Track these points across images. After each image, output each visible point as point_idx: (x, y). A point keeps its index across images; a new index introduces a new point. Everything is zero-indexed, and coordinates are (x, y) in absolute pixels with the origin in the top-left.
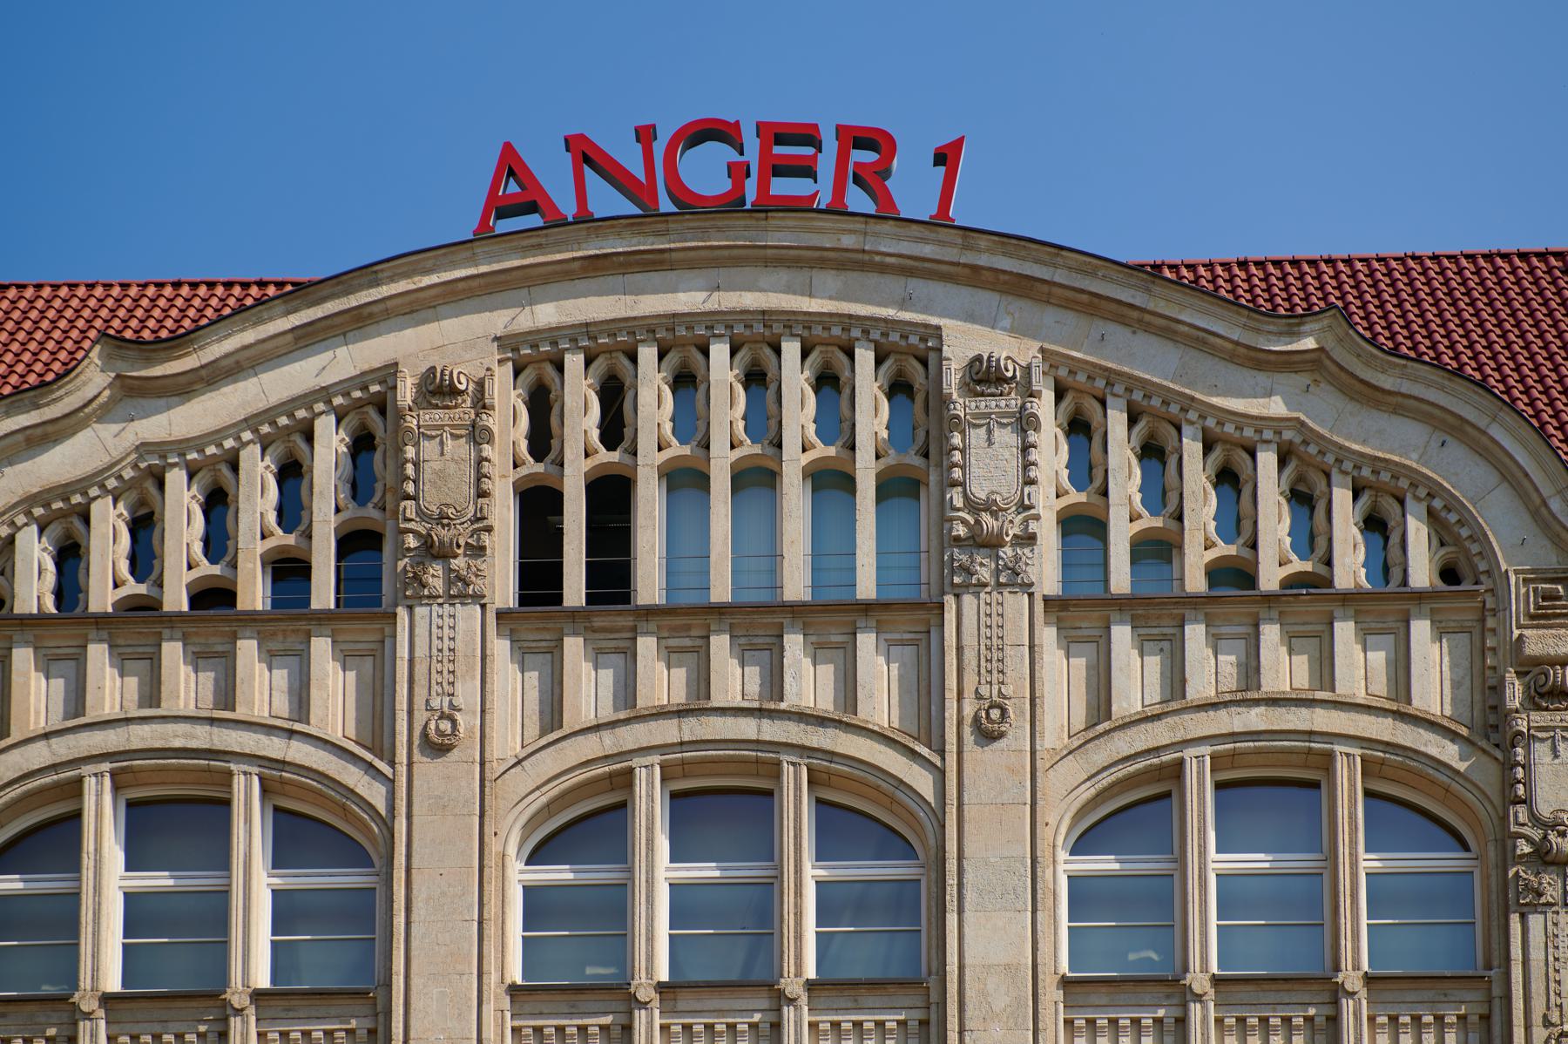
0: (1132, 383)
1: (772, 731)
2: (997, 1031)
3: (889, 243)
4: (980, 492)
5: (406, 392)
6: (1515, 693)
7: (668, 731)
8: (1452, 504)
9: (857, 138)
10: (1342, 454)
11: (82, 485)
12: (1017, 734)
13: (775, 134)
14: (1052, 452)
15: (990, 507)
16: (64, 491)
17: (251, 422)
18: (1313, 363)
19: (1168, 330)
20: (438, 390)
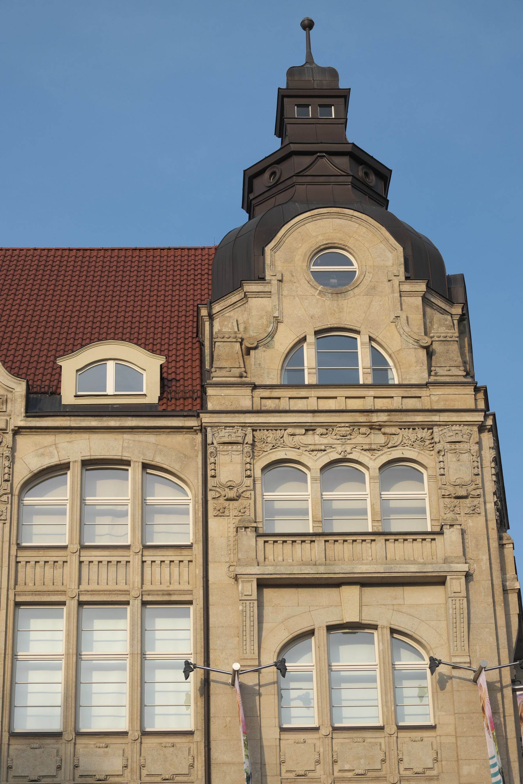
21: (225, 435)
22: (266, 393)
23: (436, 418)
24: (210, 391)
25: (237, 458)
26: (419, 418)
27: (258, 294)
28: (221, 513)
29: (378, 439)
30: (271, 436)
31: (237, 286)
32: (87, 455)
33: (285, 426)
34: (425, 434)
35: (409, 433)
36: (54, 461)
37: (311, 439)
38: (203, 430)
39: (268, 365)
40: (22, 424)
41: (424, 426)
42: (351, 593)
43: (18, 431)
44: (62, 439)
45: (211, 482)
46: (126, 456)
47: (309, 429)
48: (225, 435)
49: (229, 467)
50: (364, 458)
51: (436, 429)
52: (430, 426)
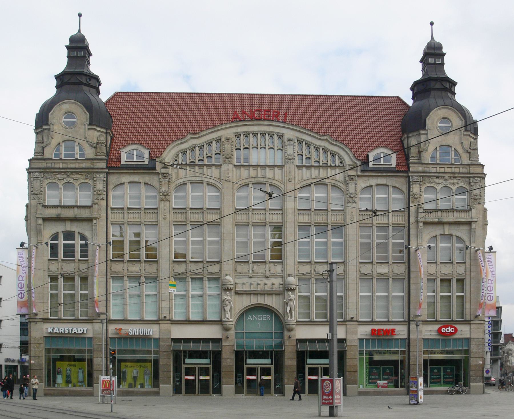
0: (306, 141)
1: (265, 180)
2: (290, 215)
3: (278, 124)
4: (289, 153)
5: (223, 140)
6: (347, 179)
7: (253, 180)
8: (341, 156)
9: (274, 112)
10: (329, 150)
11: (186, 149)
12: (293, 182)
13: (266, 111)
14: (297, 148)
15: (290, 155)
16: (184, 149)
17: (205, 142)
18: (326, 140)
19: (310, 135)
20: (228, 140)
21: (415, 179)
22: (425, 166)
23: (471, 175)
24: (411, 165)
25: (418, 186)
26: (467, 175)
27: (423, 134)
28: (413, 202)
29: (455, 181)
30: (427, 179)
31: (417, 130)
32: (377, 183)
33: (430, 176)
34: (468, 180)
35: (464, 180)
36: (368, 185)
37: (437, 180)
38: (408, 177)
39: (427, 157)
40: (360, 174)
41: (467, 177)
42: (447, 227)
43: (358, 176)
44: (370, 179)
45: (411, 193)
46: (388, 184)
47: (437, 177)
48: (415, 179)
49: (415, 189)
50: (451, 187)
51: (471, 179)
52: (469, 177)
